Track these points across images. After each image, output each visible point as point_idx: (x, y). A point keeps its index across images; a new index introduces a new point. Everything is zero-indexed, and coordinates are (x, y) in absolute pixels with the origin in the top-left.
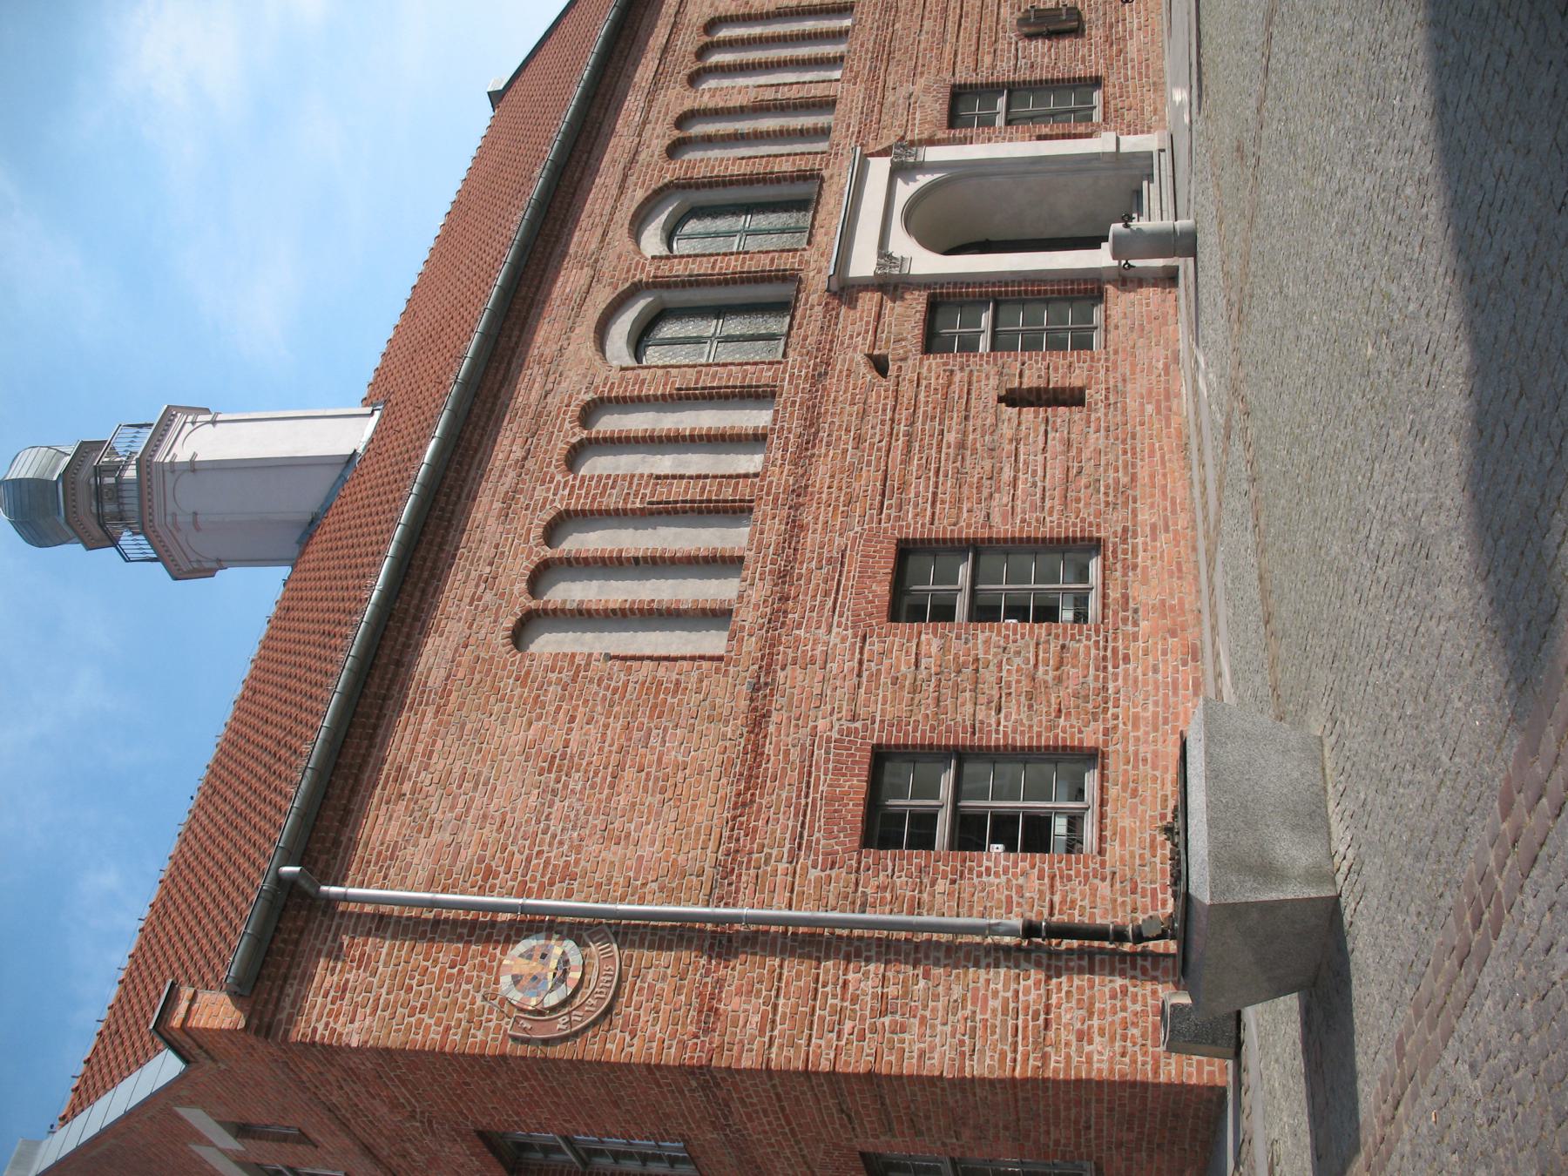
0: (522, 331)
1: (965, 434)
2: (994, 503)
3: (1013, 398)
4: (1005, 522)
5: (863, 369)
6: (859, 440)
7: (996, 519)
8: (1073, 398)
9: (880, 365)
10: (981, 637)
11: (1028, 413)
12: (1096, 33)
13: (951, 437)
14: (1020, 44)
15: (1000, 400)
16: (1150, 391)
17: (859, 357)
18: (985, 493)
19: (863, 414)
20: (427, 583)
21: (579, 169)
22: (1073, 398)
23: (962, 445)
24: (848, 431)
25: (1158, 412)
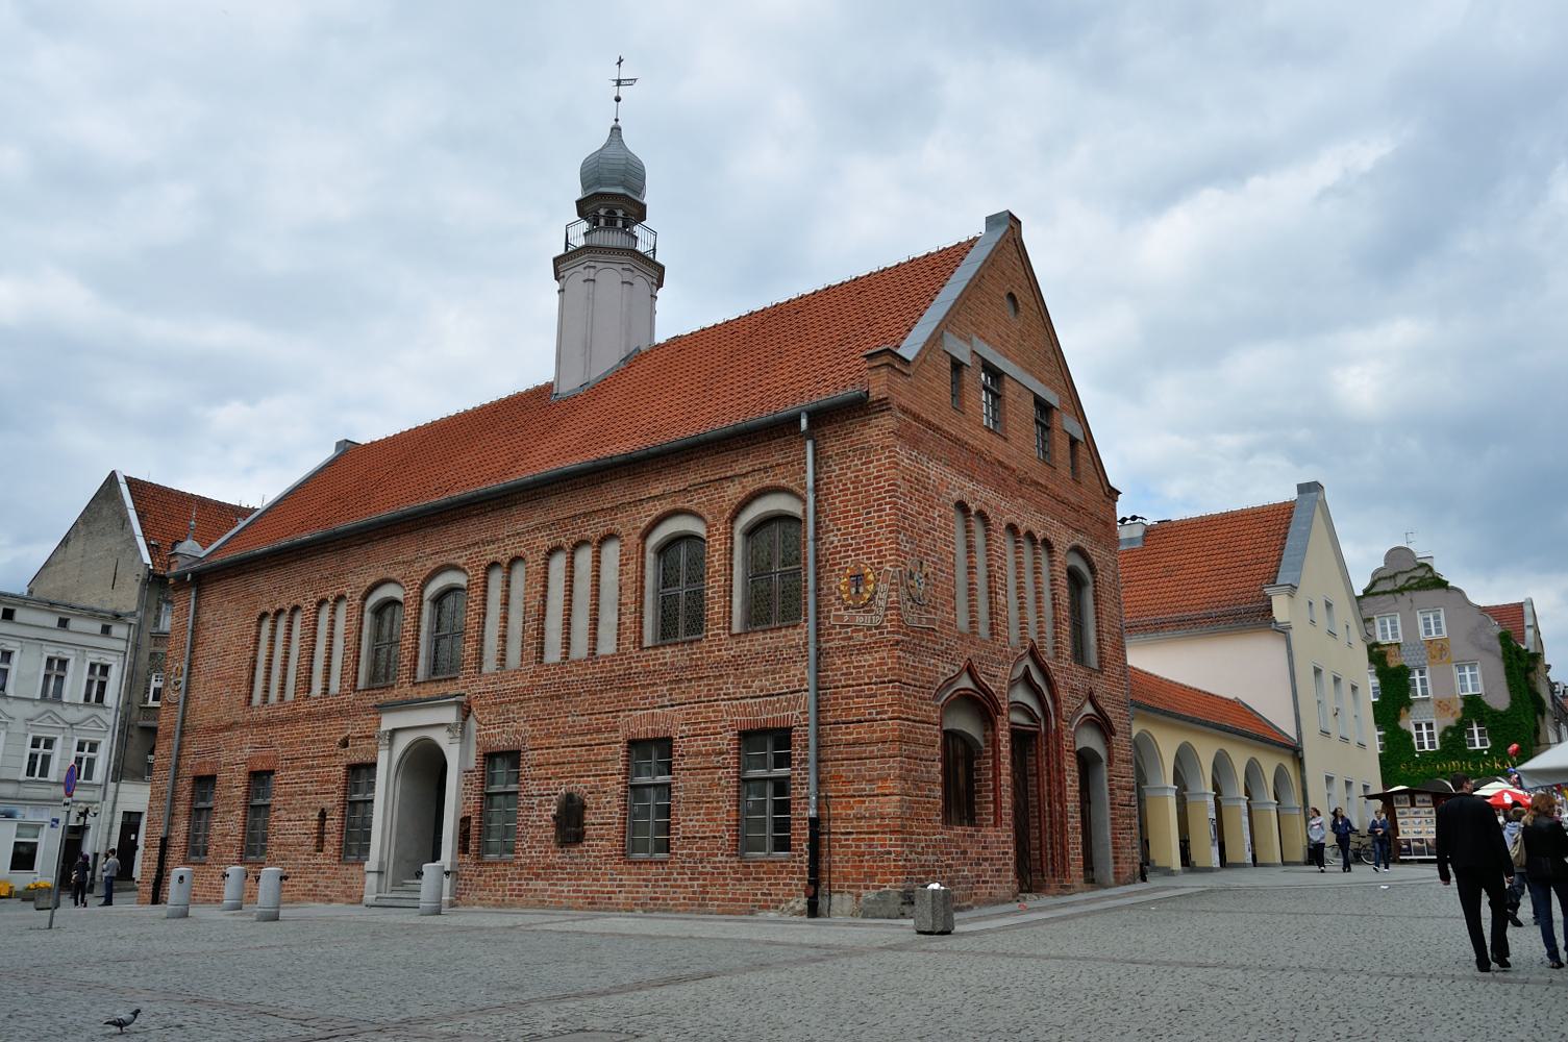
0: (380, 539)
1: (310, 794)
2: (283, 812)
3: (323, 815)
4: (276, 817)
5: (342, 736)
6: (313, 742)
7: (276, 814)
8: (320, 847)
9: (345, 744)
10: (240, 812)
11: (315, 824)
12: (555, 858)
13: (309, 788)
14: (554, 797)
15: (323, 809)
16: (318, 886)
17: (349, 731)
18: (287, 807)
19: (325, 741)
20: (280, 564)
21: (478, 512)
22: (320, 847)
23: (305, 793)
24: (317, 735)
25: (309, 890)
